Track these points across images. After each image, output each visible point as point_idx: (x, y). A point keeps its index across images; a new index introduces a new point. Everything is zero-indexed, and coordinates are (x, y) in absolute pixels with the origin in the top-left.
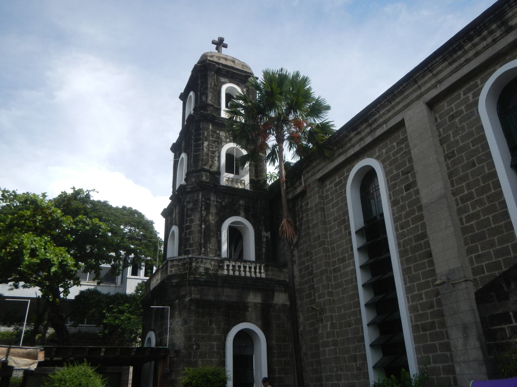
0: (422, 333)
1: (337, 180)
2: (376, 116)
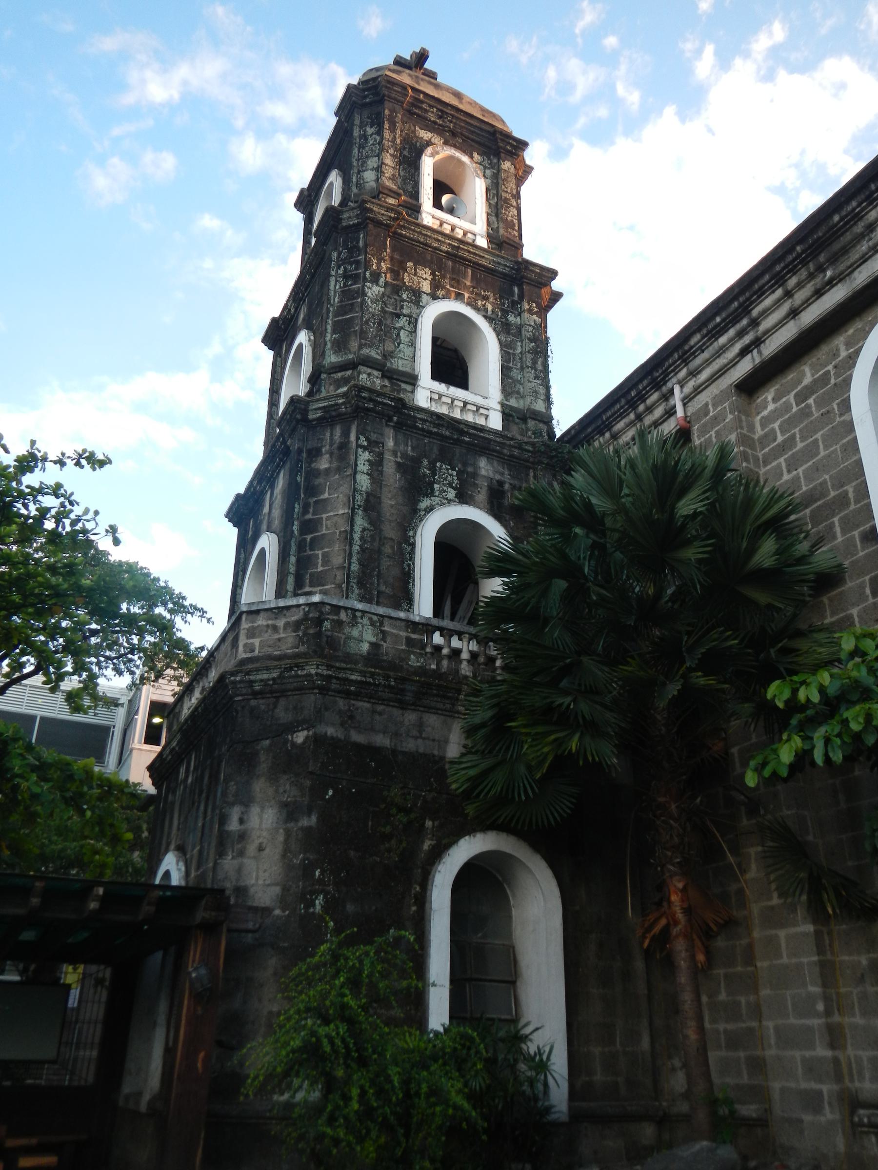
1: (808, 380)
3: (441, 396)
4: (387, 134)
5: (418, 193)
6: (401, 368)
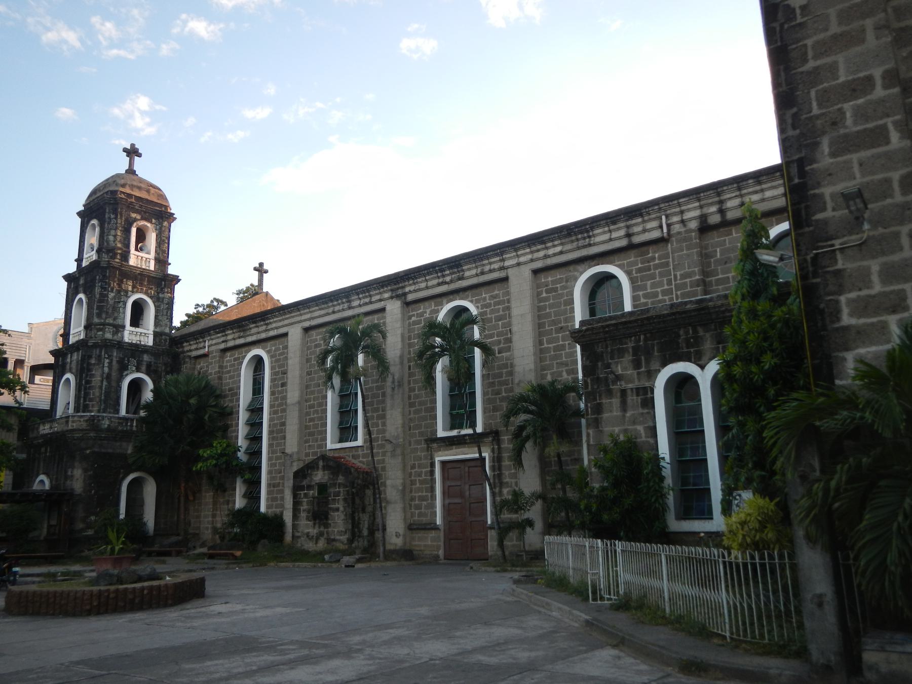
0: (272, 489)
1: (236, 356)
2: (272, 321)
3: (133, 332)
4: (119, 221)
6: (120, 324)
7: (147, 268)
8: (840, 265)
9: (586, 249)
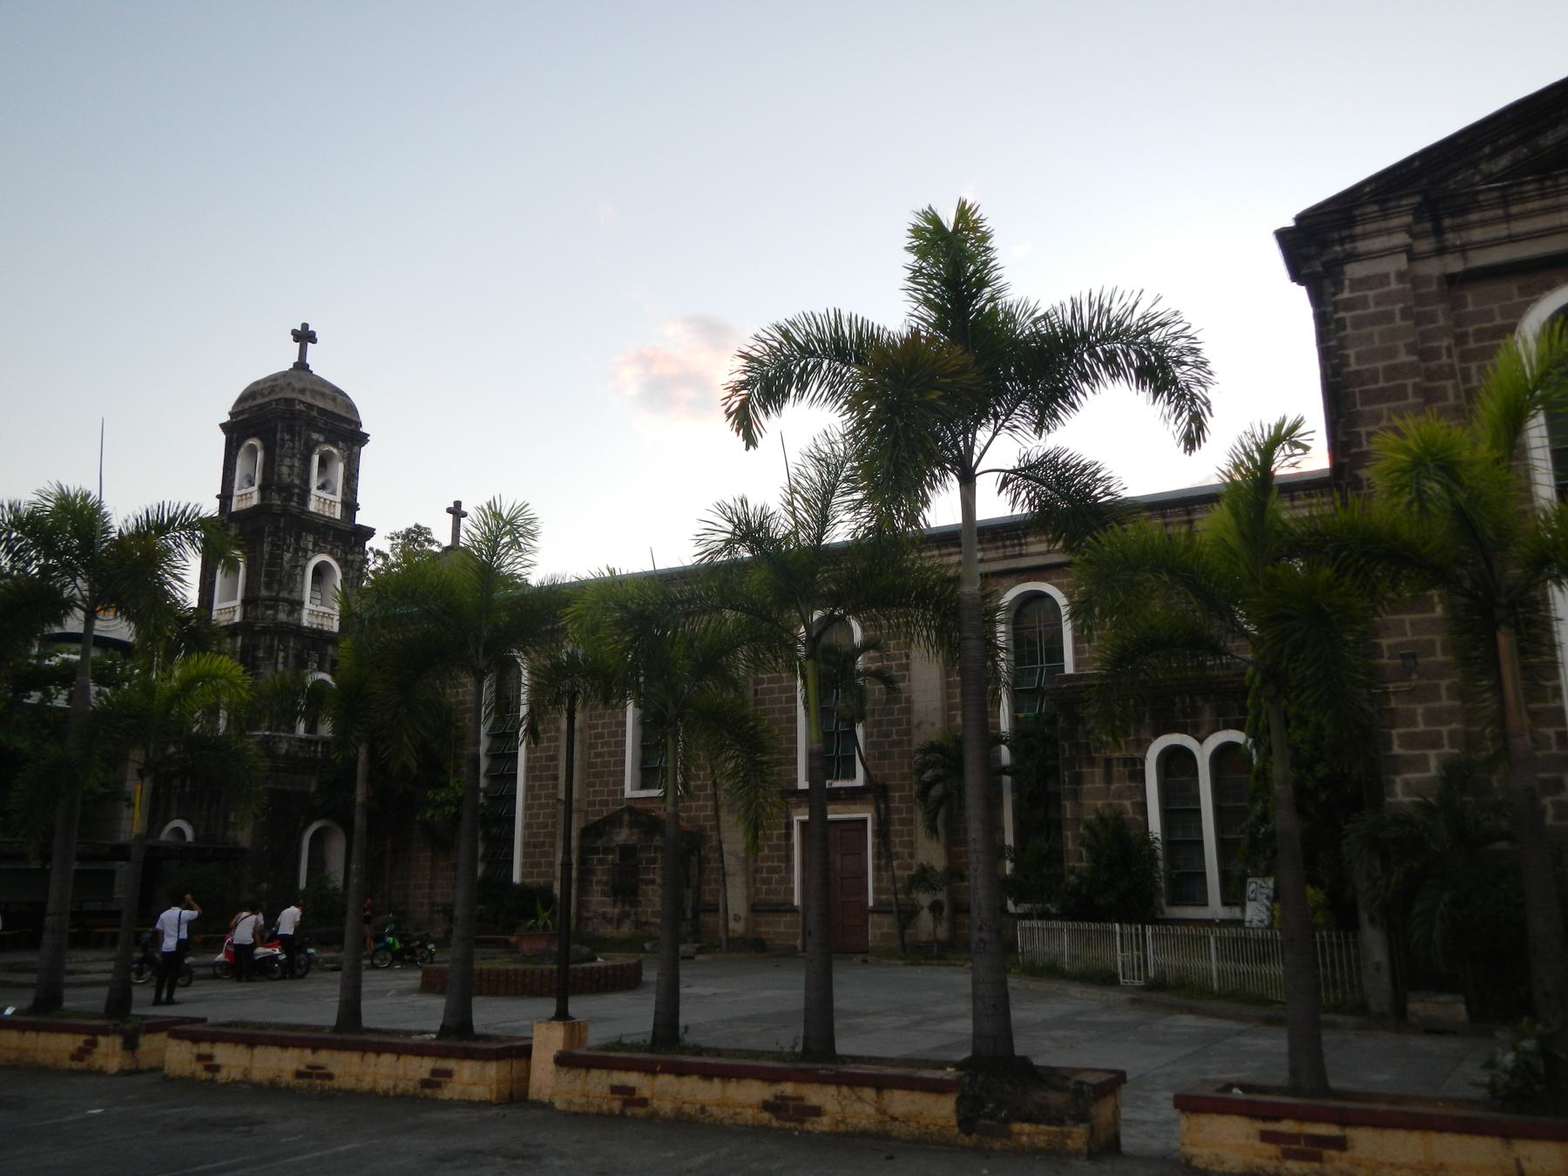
3: (313, 611)
5: (309, 478)
7: (332, 516)
8: (1393, 704)
9: (1015, 560)
